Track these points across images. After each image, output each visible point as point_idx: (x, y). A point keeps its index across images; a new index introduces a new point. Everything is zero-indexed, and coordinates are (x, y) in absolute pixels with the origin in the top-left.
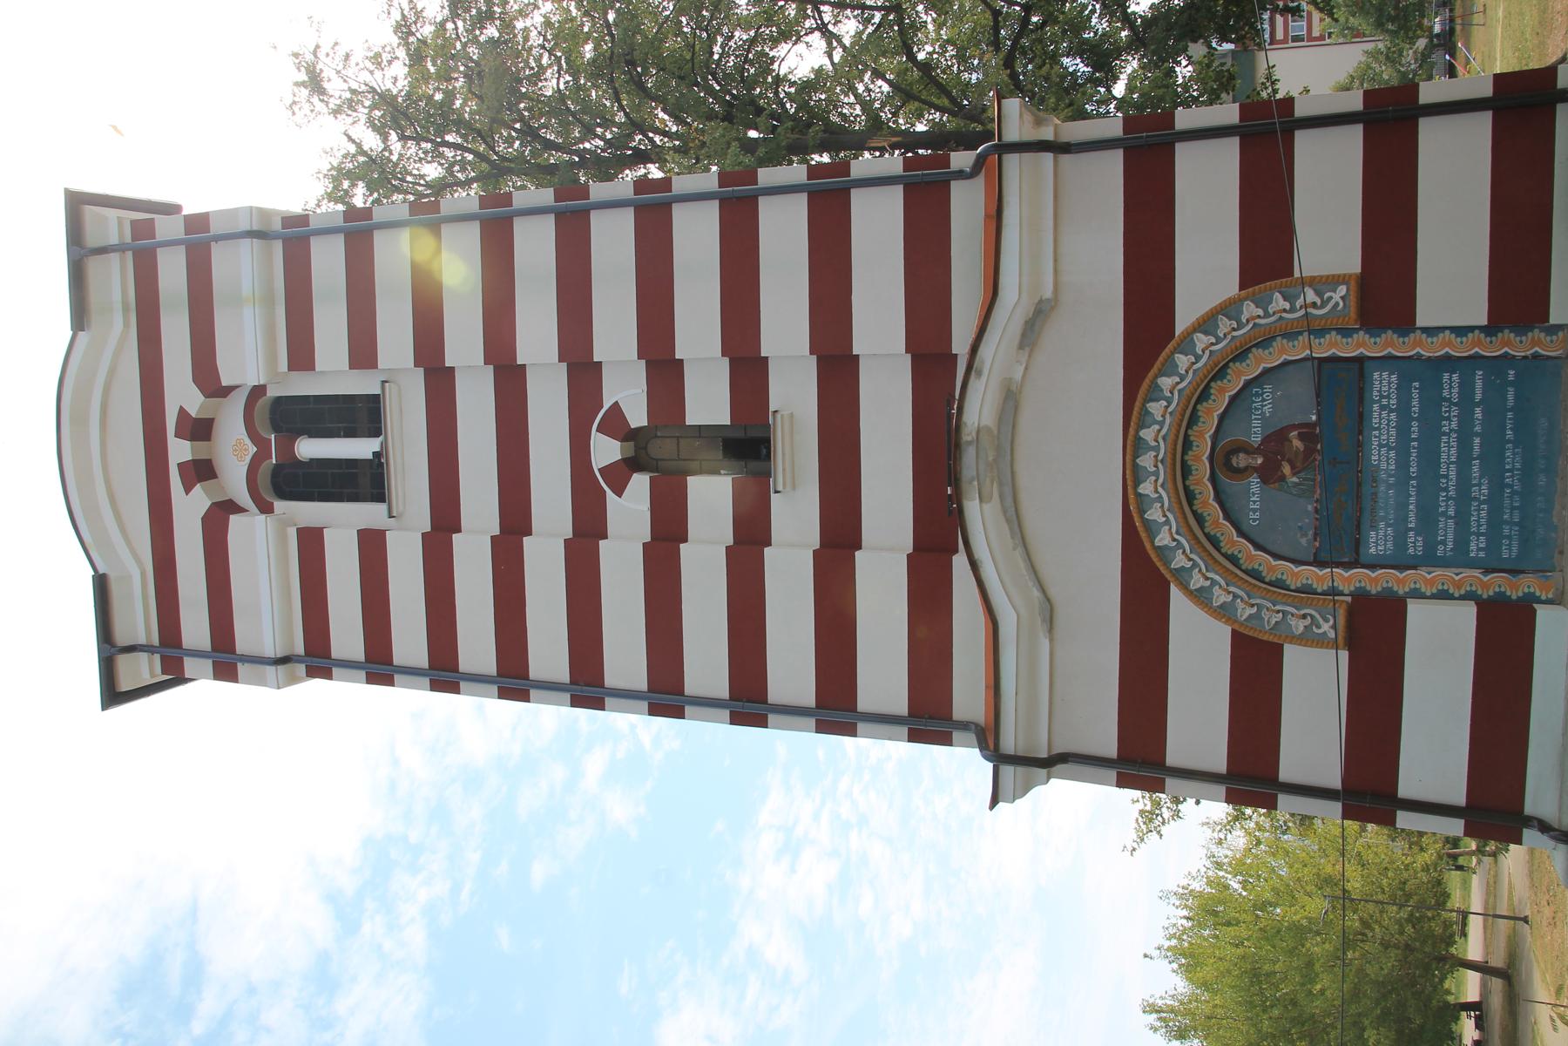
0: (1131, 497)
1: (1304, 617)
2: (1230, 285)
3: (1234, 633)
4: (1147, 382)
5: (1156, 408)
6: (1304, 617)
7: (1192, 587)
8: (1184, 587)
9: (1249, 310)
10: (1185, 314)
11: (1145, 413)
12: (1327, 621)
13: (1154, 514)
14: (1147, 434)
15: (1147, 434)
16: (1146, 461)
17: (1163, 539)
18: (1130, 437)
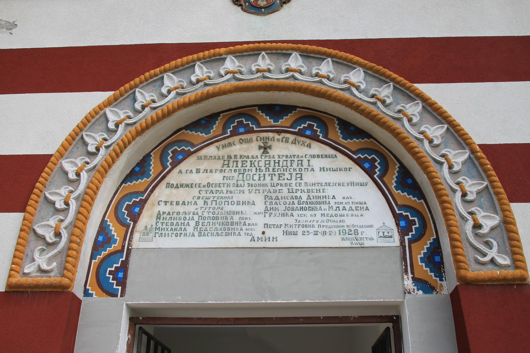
0: (223, 50)
1: (58, 234)
2: (482, 134)
3: (51, 156)
4: (356, 58)
5: (326, 68)
6: (58, 234)
7: (108, 110)
8: (109, 103)
9: (459, 158)
10: (442, 93)
11: (320, 57)
12: (50, 261)
13: (200, 71)
14: (295, 61)
15: (295, 61)
16: (263, 62)
17: (170, 81)
18: (290, 45)
